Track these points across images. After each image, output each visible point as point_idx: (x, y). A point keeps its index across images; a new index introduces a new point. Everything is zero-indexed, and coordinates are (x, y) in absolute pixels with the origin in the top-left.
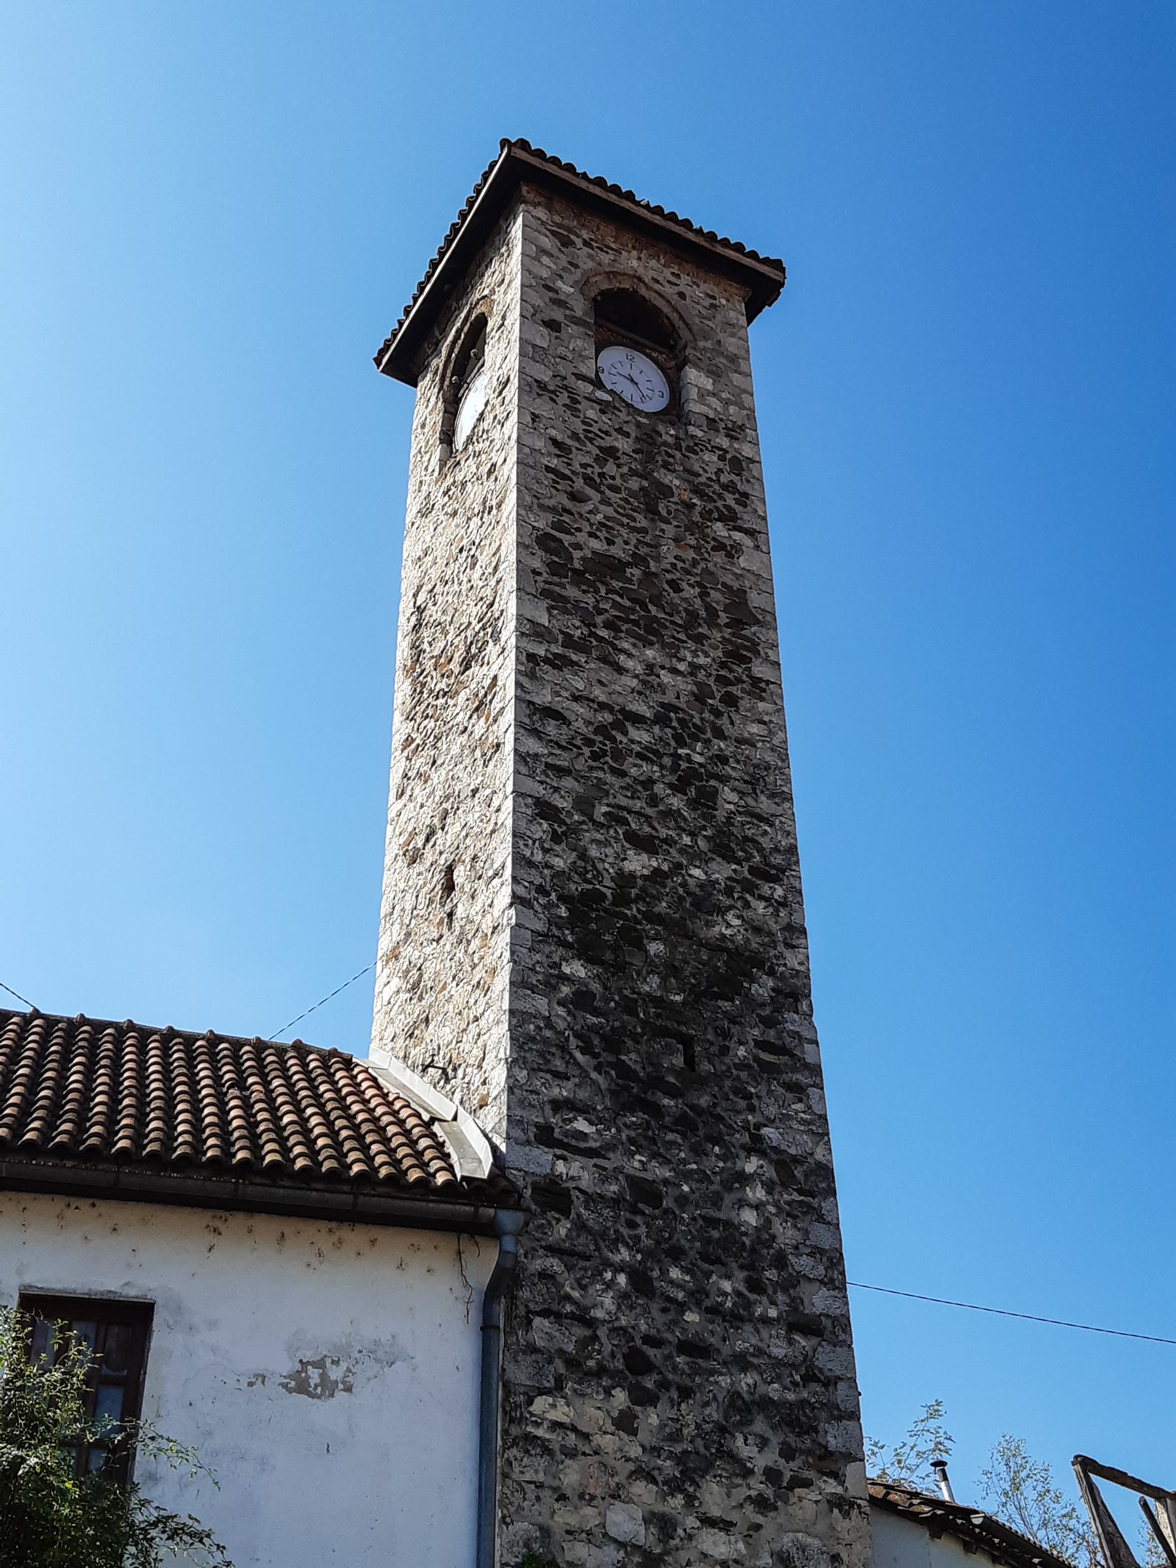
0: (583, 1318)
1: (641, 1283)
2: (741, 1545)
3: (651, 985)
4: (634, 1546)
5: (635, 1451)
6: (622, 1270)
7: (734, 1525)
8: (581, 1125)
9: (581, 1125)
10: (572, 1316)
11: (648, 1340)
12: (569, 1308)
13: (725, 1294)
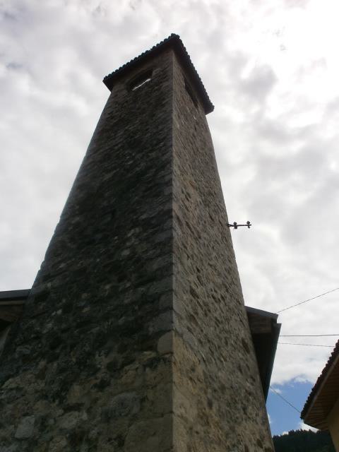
0: (38, 337)
1: (67, 308)
2: (85, 416)
3: (105, 203)
4: (26, 439)
5: (41, 385)
6: (61, 308)
7: (82, 404)
8: (62, 265)
9: (62, 265)
10: (35, 338)
11: (64, 331)
12: (32, 336)
13: (106, 291)
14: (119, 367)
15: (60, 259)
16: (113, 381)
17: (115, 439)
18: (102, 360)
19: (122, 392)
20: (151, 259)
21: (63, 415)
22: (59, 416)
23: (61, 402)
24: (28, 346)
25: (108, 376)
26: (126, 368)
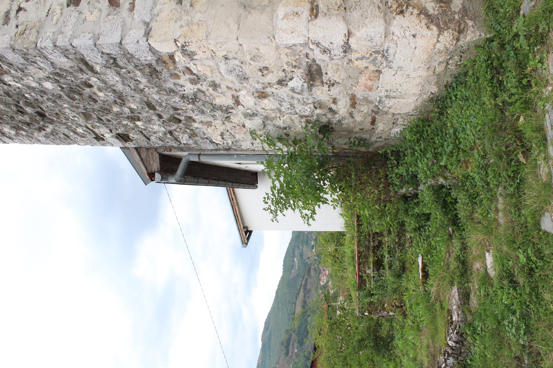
14: (195, 76)
15: (72, 134)
16: (210, 79)
17: (263, 73)
18: (189, 89)
19: (220, 72)
20: (51, 63)
21: (242, 105)
22: (244, 107)
23: (232, 108)
24: (180, 137)
25: (205, 83)
26: (195, 72)
